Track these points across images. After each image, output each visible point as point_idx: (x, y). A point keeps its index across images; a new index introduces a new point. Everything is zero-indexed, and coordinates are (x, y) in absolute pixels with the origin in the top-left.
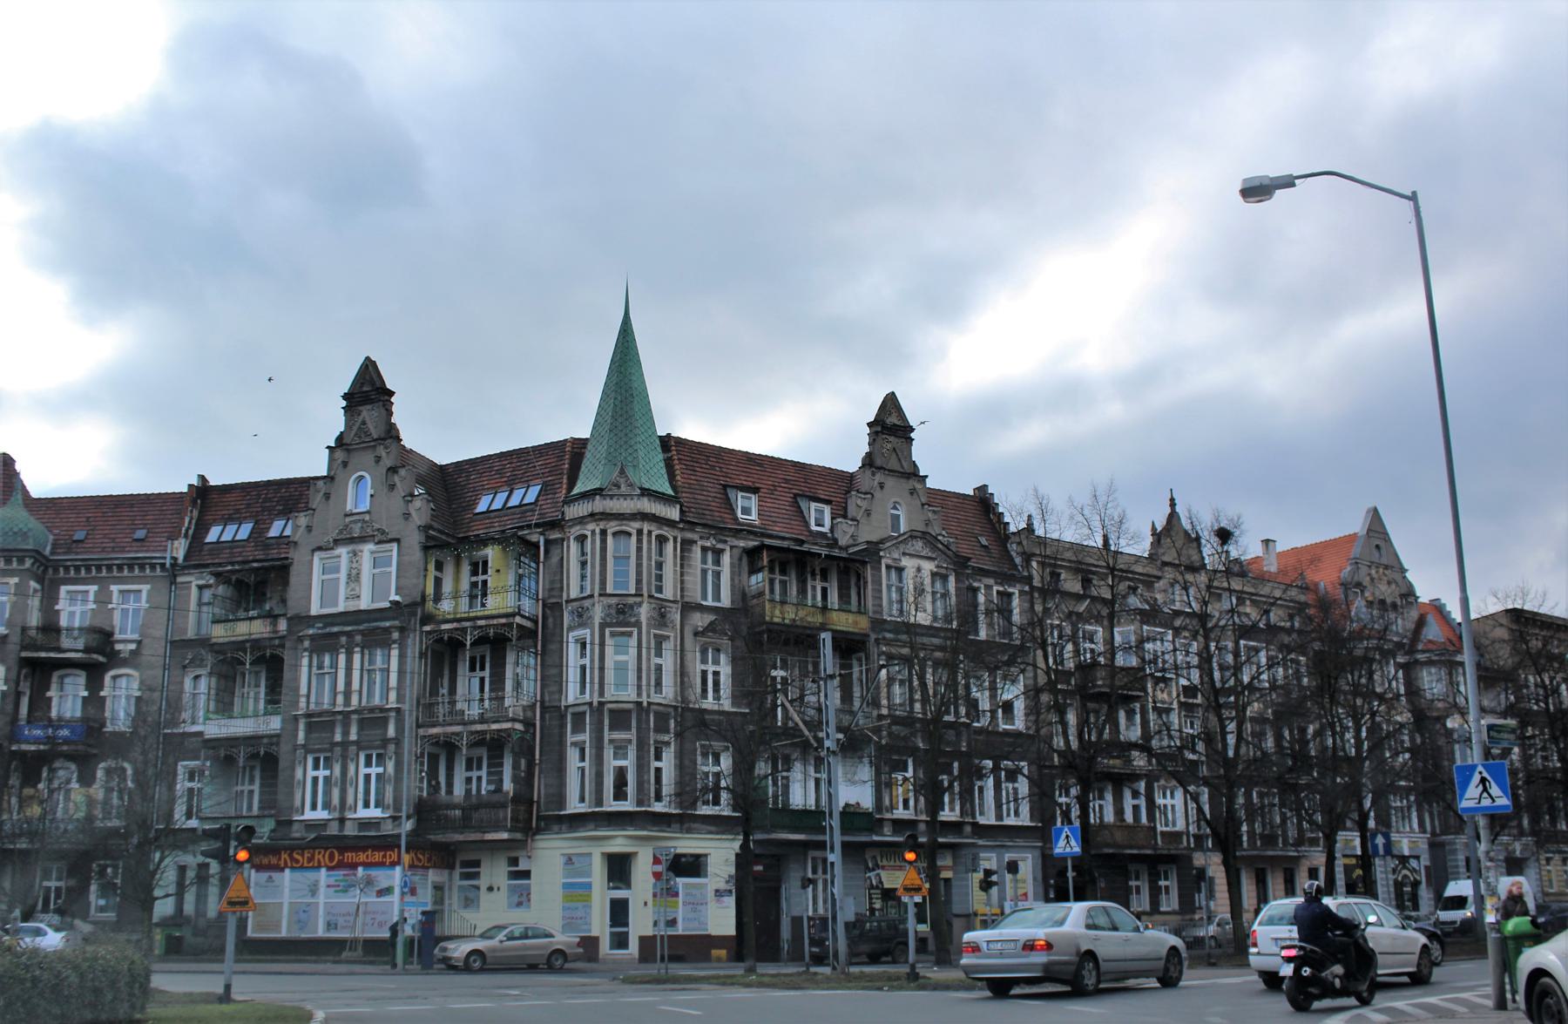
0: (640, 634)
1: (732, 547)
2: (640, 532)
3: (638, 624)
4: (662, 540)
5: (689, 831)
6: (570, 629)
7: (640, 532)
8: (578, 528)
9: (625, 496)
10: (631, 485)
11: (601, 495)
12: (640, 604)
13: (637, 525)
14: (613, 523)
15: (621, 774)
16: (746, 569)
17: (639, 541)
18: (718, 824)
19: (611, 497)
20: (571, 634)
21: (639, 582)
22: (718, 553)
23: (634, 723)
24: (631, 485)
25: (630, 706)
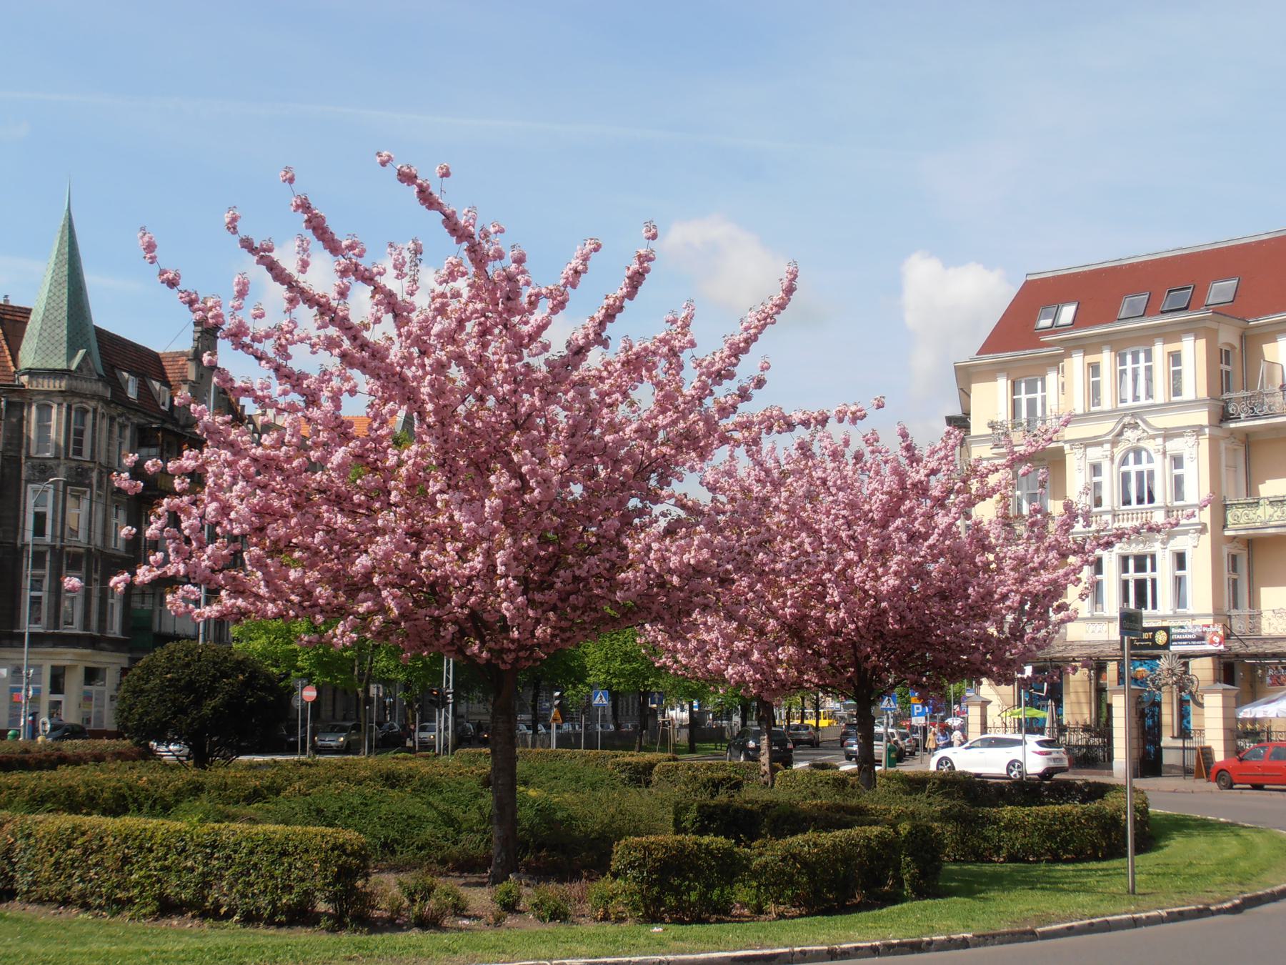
0: (91, 493)
1: (132, 424)
2: (95, 411)
3: (90, 486)
4: (84, 412)
5: (102, 649)
6: (28, 481)
7: (95, 411)
8: (42, 397)
9: (86, 380)
10: (90, 370)
11: (70, 375)
12: (92, 470)
13: (93, 403)
14: (77, 400)
15: (36, 601)
16: (136, 444)
17: (94, 418)
18: (116, 645)
19: (76, 378)
20: (30, 486)
21: (93, 451)
22: (122, 427)
23: (84, 565)
24: (90, 370)
25: (82, 550)
